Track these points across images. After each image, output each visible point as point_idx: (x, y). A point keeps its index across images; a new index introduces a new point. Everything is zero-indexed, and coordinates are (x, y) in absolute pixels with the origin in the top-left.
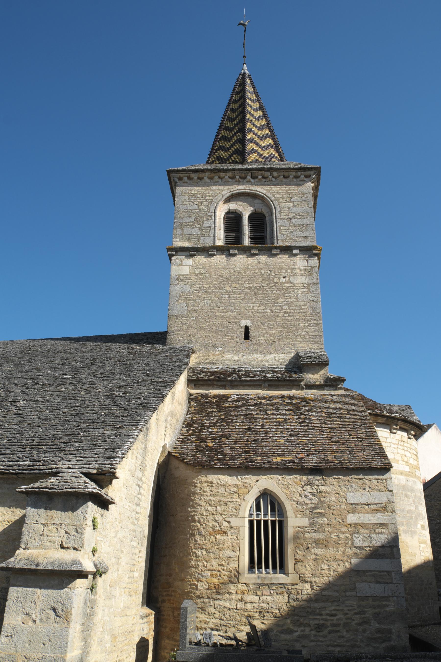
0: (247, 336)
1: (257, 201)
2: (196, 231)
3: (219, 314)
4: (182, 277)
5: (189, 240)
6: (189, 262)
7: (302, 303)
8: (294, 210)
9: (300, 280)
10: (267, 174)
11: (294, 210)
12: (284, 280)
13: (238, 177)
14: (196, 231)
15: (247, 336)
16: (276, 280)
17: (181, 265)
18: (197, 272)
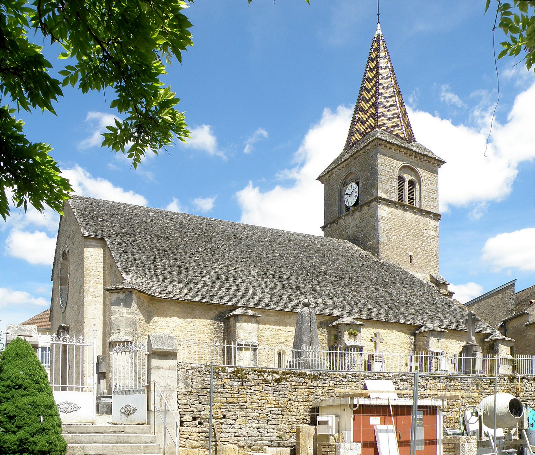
0: (411, 262)
1: (413, 173)
2: (388, 187)
3: (400, 246)
4: (384, 218)
5: (385, 193)
6: (386, 208)
7: (432, 247)
8: (430, 186)
9: (432, 233)
10: (422, 157)
11: (430, 186)
12: (425, 232)
13: (408, 154)
14: (388, 187)
15: (411, 262)
16: (423, 231)
17: (383, 209)
18: (390, 216)
